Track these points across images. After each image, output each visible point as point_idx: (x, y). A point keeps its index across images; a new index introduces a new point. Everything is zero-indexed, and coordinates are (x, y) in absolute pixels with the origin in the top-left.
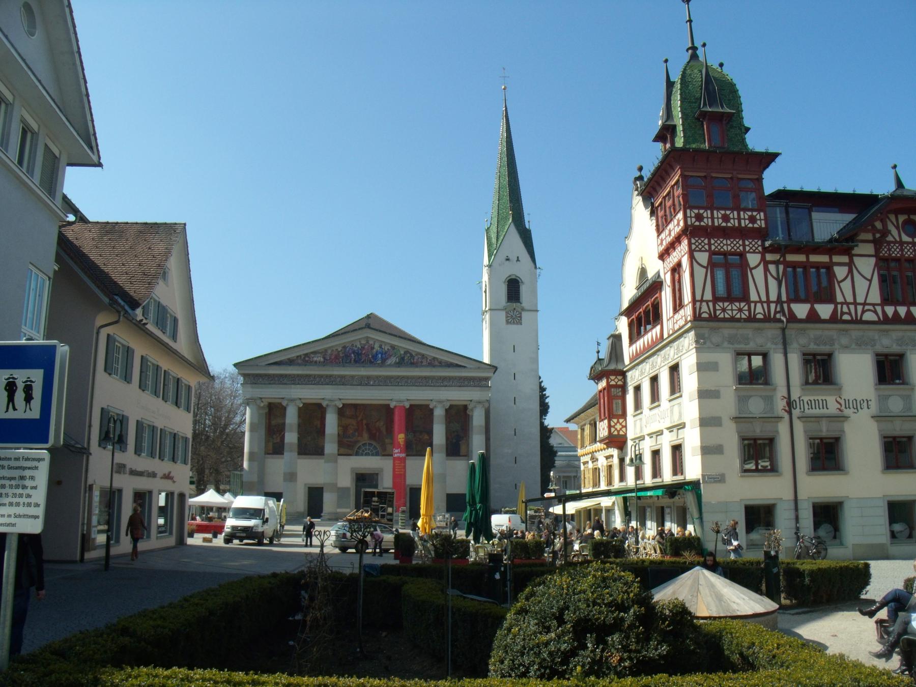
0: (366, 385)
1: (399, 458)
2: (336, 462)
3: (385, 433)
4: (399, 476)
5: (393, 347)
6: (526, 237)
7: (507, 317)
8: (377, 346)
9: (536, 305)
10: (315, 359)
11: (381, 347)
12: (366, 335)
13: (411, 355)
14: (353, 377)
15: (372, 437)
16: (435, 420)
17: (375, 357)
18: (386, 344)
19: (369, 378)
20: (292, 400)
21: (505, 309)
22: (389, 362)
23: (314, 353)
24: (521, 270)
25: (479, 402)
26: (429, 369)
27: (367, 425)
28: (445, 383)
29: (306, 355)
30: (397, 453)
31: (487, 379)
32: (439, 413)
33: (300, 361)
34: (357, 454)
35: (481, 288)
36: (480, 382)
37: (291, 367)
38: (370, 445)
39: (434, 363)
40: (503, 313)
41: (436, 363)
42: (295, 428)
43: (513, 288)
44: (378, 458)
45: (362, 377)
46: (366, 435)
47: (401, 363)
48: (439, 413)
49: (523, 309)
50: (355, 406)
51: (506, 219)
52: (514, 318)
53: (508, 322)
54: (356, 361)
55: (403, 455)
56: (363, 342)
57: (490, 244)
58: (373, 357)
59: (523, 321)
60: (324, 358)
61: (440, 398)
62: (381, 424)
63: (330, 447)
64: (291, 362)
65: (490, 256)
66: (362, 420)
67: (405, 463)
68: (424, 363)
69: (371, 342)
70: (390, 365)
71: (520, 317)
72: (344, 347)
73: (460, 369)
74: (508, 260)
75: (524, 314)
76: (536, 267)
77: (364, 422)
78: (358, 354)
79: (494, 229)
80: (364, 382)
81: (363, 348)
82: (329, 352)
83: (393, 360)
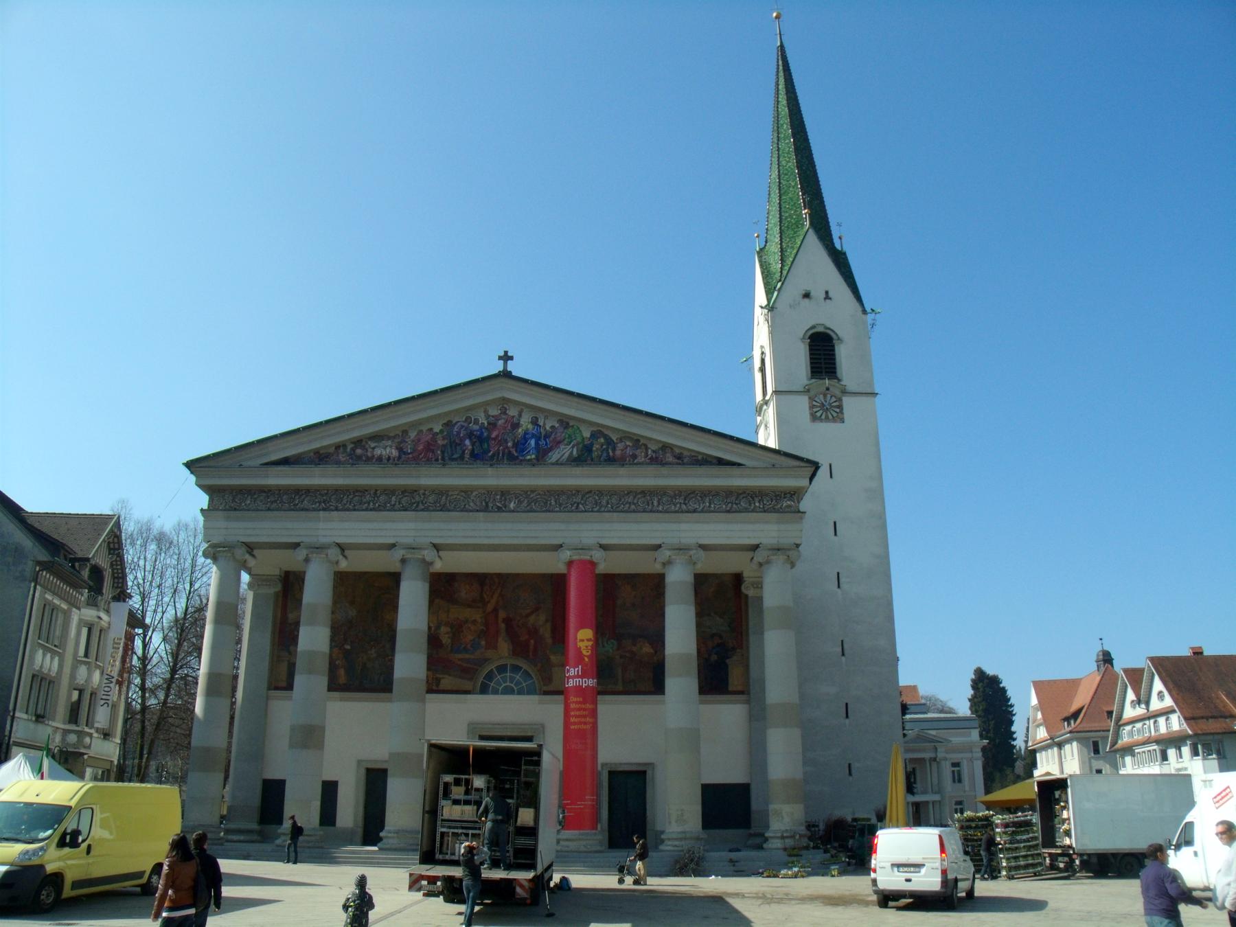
0: (499, 509)
1: (579, 690)
2: (423, 701)
3: (549, 641)
4: (581, 738)
5: (565, 422)
6: (840, 261)
7: (812, 407)
8: (526, 423)
9: (871, 383)
10: (378, 452)
11: (535, 422)
12: (498, 395)
13: (609, 441)
14: (466, 491)
15: (520, 649)
16: (670, 595)
17: (521, 445)
18: (548, 413)
19: (505, 493)
20: (320, 548)
21: (807, 391)
22: (554, 456)
23: (377, 437)
24: (837, 315)
25: (778, 549)
26: (651, 469)
27: (508, 621)
28: (692, 505)
29: (358, 442)
30: (574, 677)
31: (795, 494)
32: (678, 577)
33: (342, 457)
34: (484, 690)
35: (751, 369)
36: (783, 502)
37: (317, 470)
38: (516, 669)
39: (664, 456)
40: (804, 401)
41: (670, 458)
42: (325, 615)
43: (822, 351)
44: (536, 698)
45: (489, 492)
46: (504, 646)
47: (585, 457)
48: (678, 577)
49: (844, 392)
50: (481, 580)
51: (798, 224)
52: (828, 410)
53: (814, 418)
54: (475, 456)
55: (591, 682)
56: (494, 412)
57: (767, 275)
58: (516, 445)
59: (846, 416)
60: (400, 450)
61: (679, 544)
62: (540, 621)
63: (409, 663)
64: (320, 458)
65: (769, 292)
66: (495, 610)
67: (595, 703)
68: (641, 459)
69: (513, 412)
70: (557, 463)
71: (840, 407)
72: (449, 424)
73: (728, 470)
74: (807, 295)
75: (847, 401)
76: (864, 312)
77: (502, 614)
78: (479, 439)
79: (774, 248)
80: (494, 502)
81: (493, 425)
82: (413, 435)
83: (564, 452)
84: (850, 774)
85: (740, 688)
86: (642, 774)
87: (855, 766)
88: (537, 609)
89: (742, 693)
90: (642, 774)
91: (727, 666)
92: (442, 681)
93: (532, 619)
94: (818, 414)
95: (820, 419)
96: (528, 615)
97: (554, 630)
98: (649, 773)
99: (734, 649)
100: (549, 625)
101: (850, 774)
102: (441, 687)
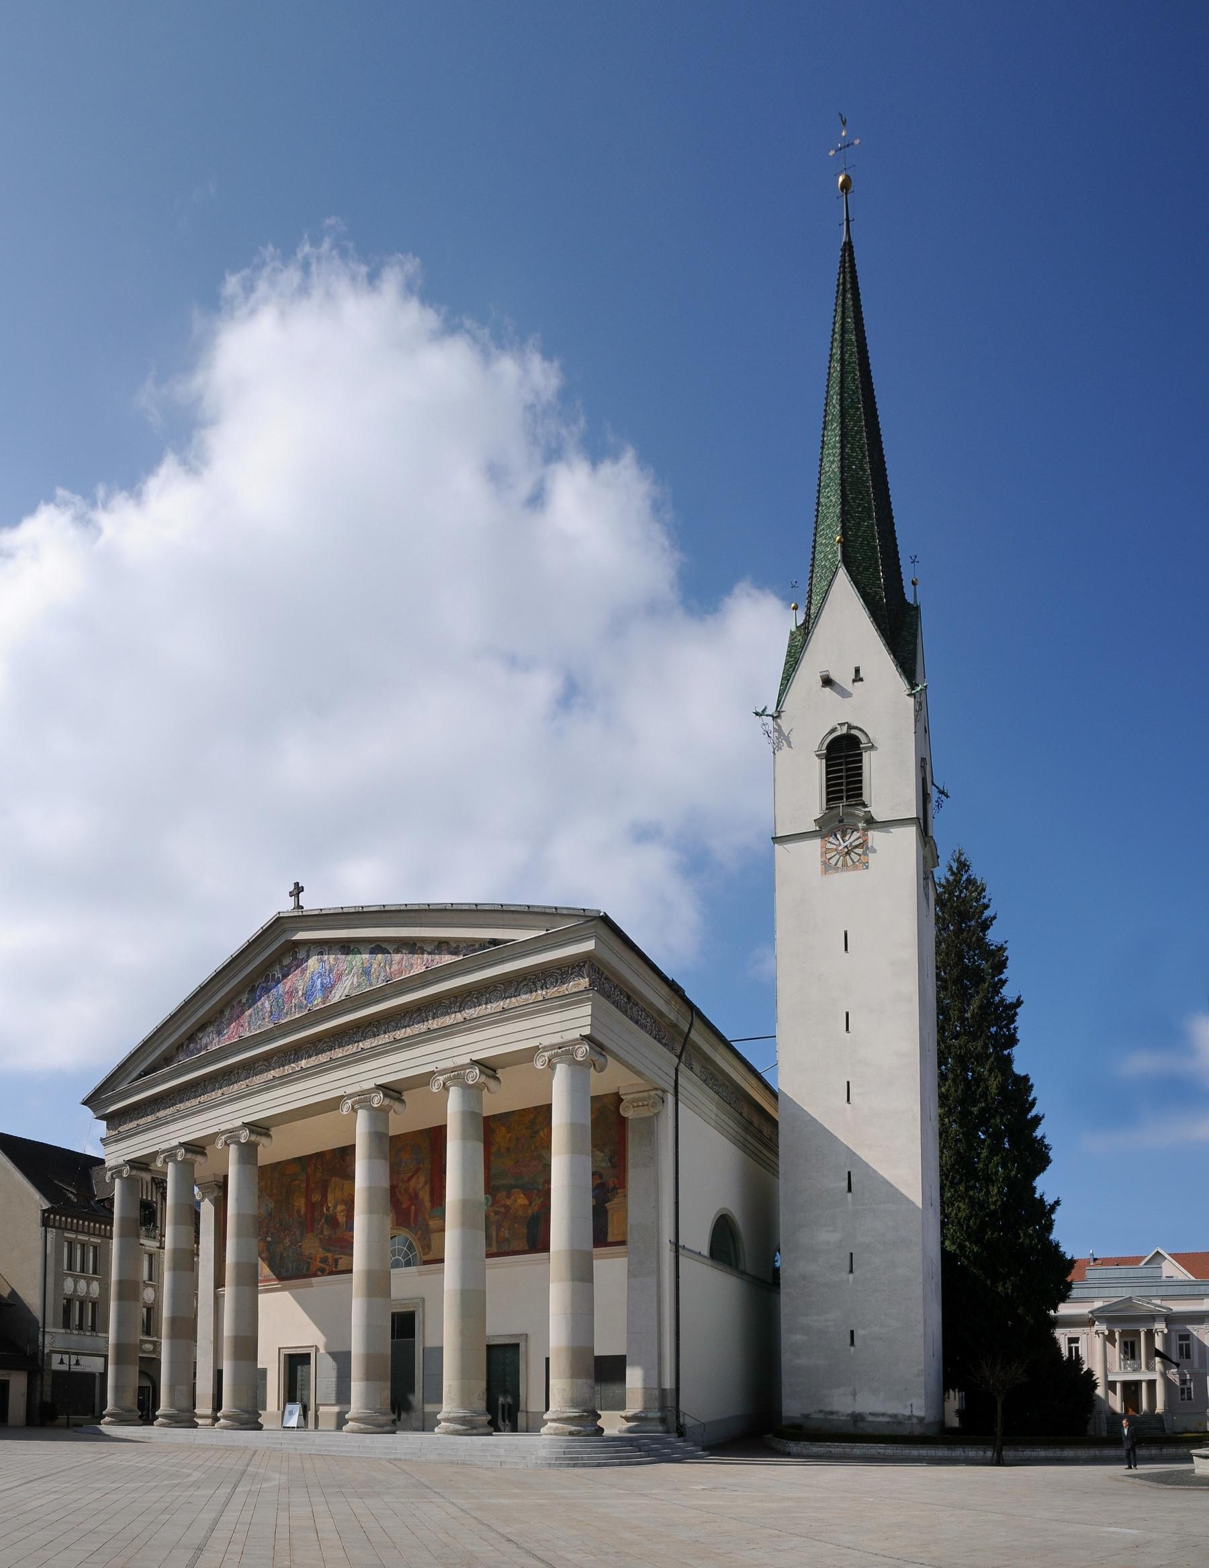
3: (428, 1205)
7: (827, 851)
49: (871, 822)
84: (852, 1343)
85: (619, 1239)
86: (516, 1346)
87: (859, 1333)
88: (416, 1172)
89: (623, 1243)
90: (516, 1346)
91: (606, 1212)
92: (340, 1262)
93: (412, 1183)
94: (833, 861)
95: (835, 868)
96: (410, 1179)
97: (432, 1193)
98: (522, 1348)
99: (614, 1188)
100: (427, 1187)
101: (852, 1343)
102: (340, 1268)
